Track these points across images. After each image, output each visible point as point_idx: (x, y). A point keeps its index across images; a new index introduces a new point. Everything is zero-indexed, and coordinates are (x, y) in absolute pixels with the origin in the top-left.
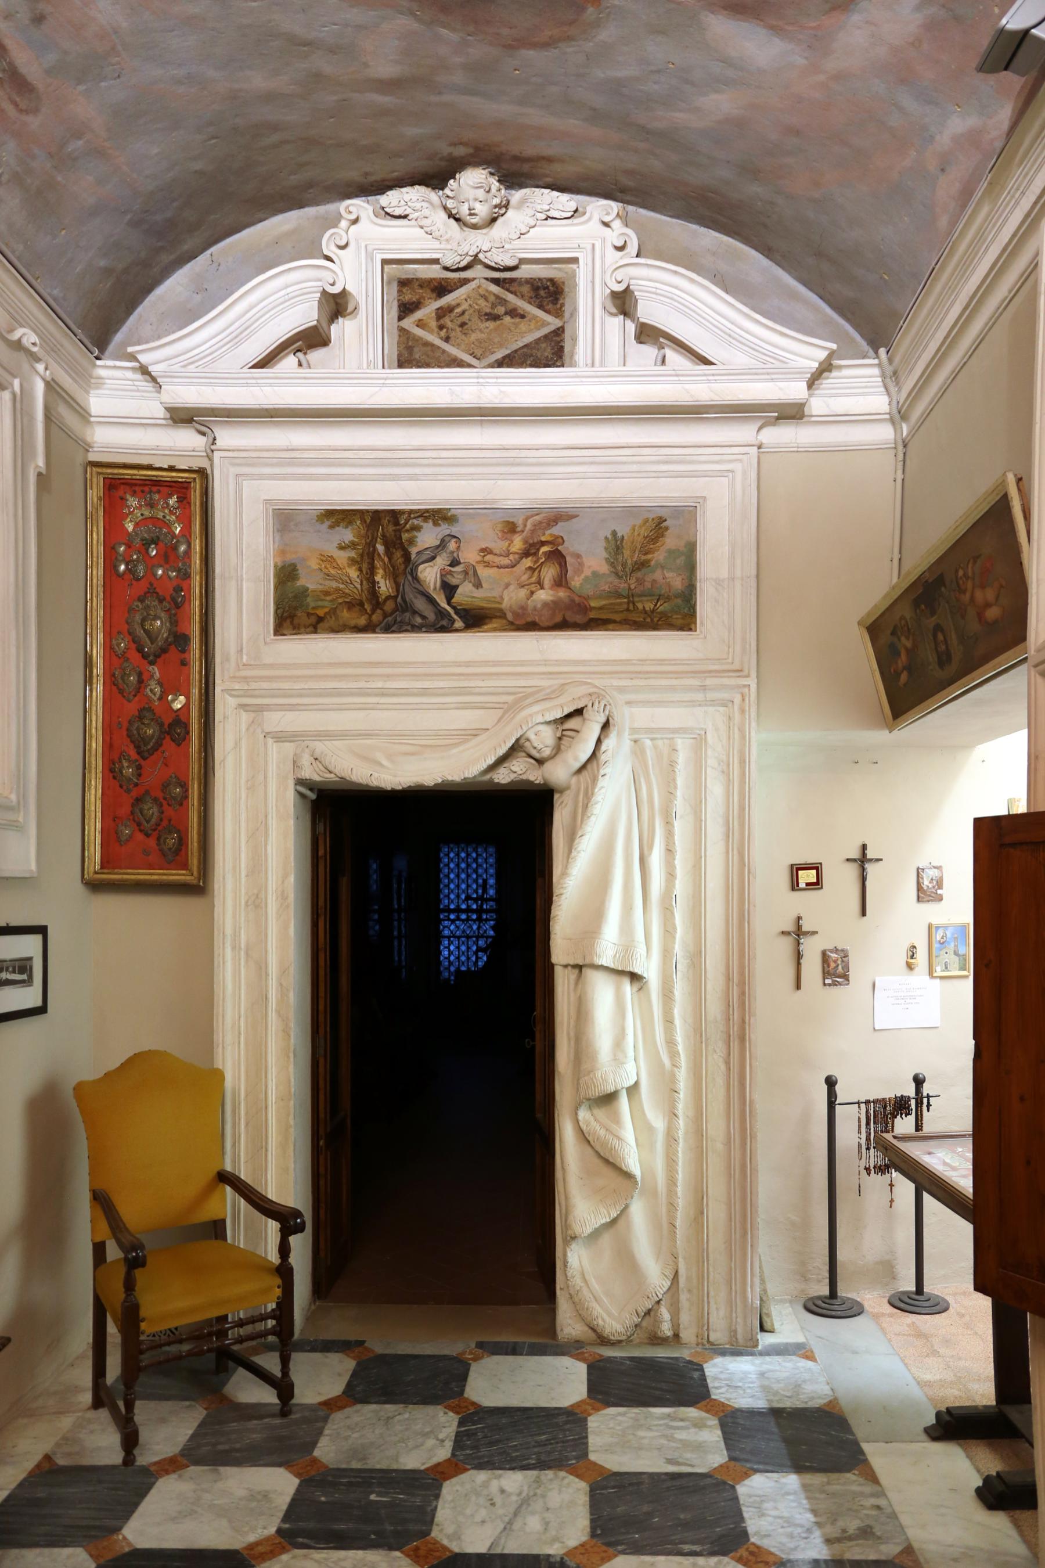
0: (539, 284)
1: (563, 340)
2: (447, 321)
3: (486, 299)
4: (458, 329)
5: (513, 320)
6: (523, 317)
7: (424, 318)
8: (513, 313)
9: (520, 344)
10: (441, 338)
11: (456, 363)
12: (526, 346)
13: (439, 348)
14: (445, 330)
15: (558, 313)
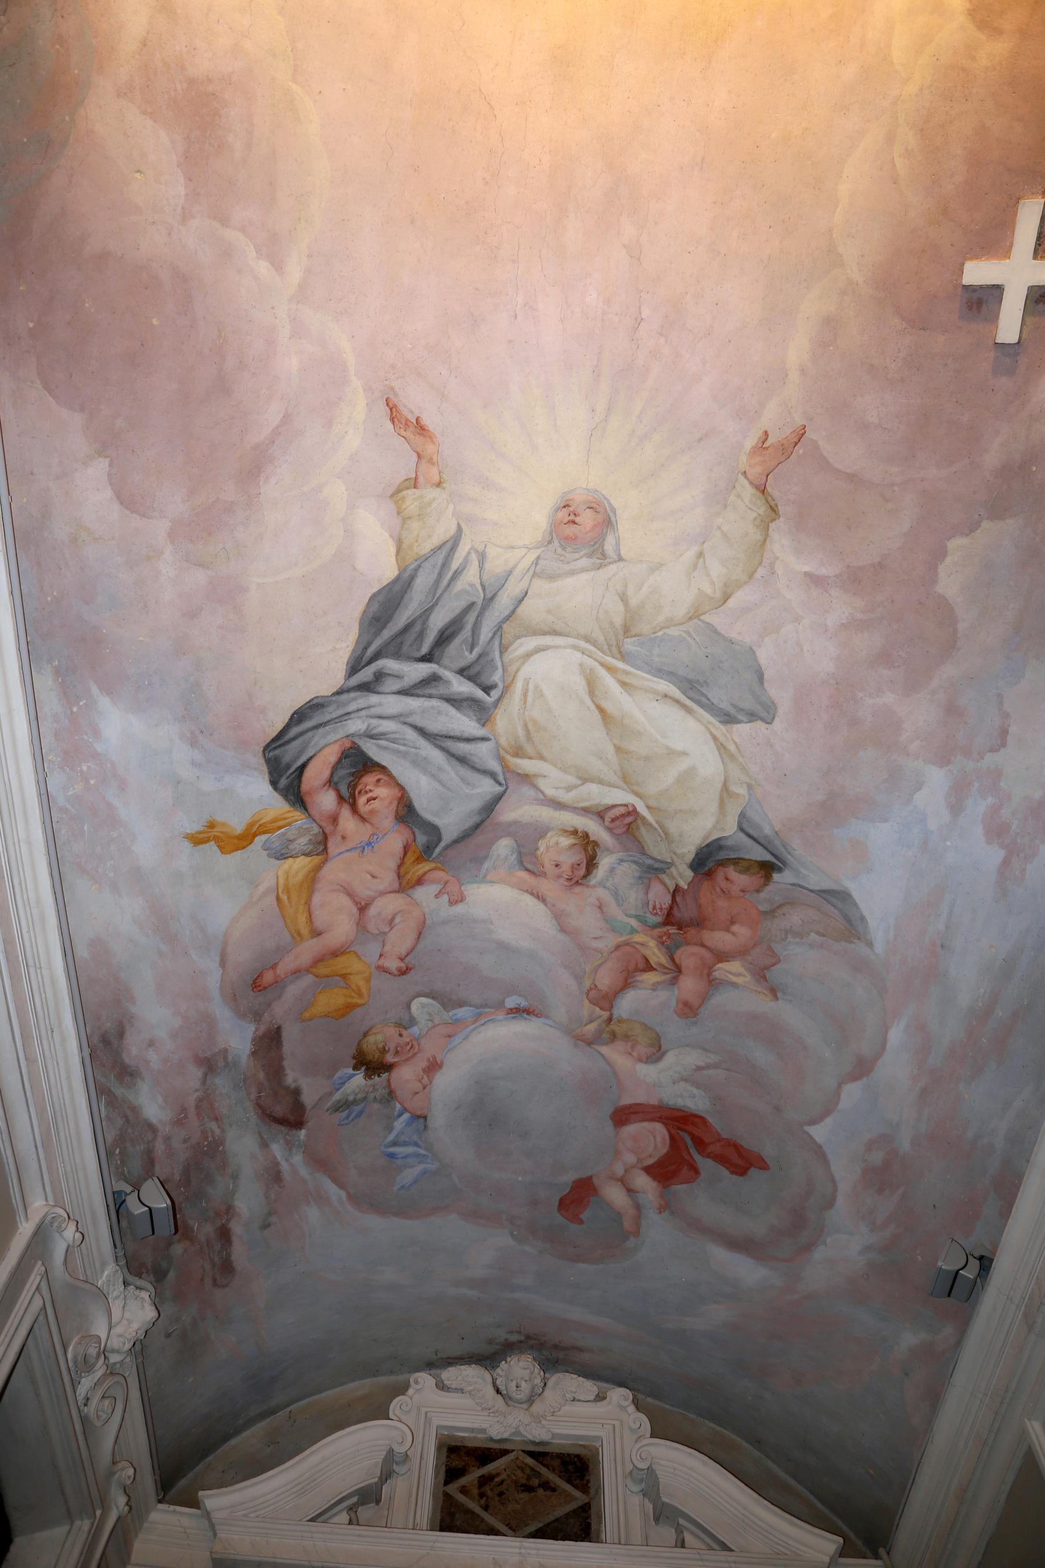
0: (568, 1460)
1: (589, 1517)
2: (487, 1489)
3: (523, 1471)
4: (497, 1499)
5: (545, 1493)
6: (554, 1490)
7: (467, 1485)
8: (546, 1485)
9: (552, 1518)
10: (481, 1506)
11: (492, 1531)
12: (556, 1520)
13: (478, 1516)
14: (485, 1498)
15: (585, 1489)
